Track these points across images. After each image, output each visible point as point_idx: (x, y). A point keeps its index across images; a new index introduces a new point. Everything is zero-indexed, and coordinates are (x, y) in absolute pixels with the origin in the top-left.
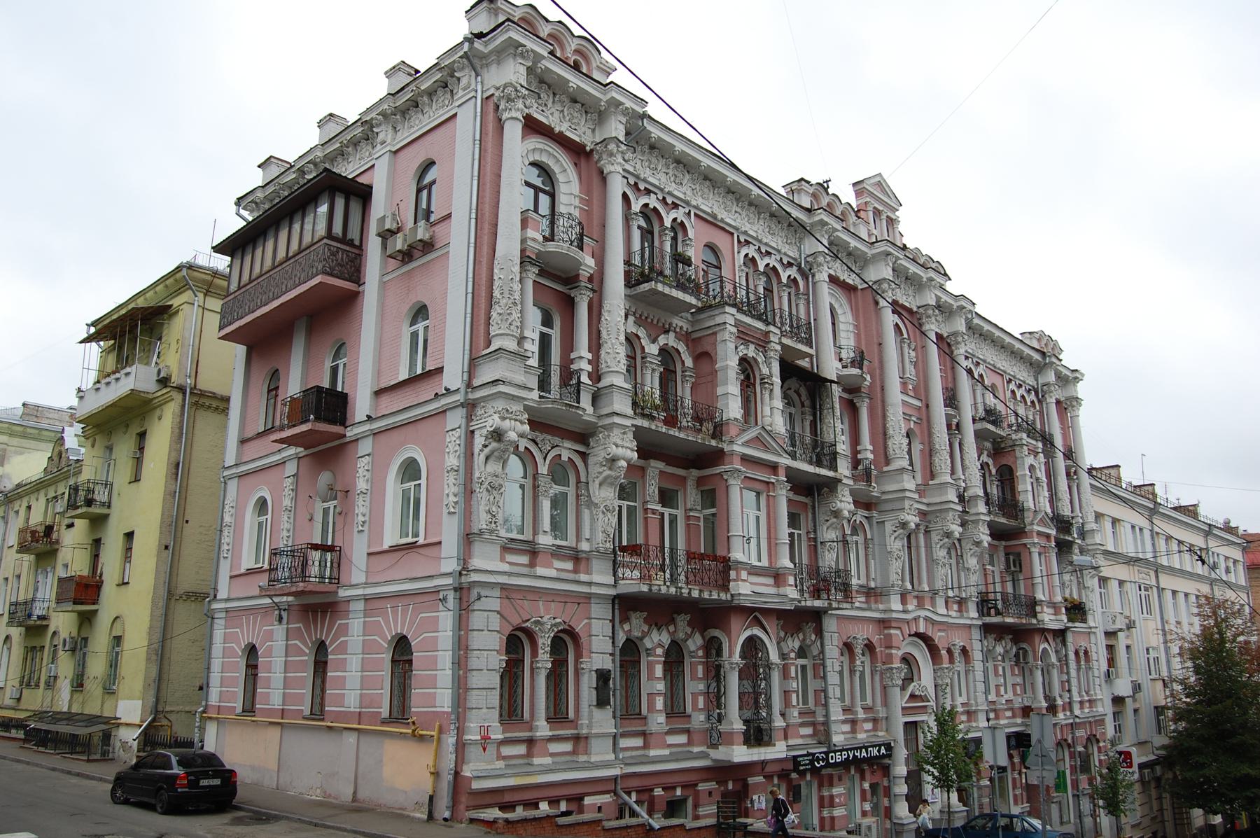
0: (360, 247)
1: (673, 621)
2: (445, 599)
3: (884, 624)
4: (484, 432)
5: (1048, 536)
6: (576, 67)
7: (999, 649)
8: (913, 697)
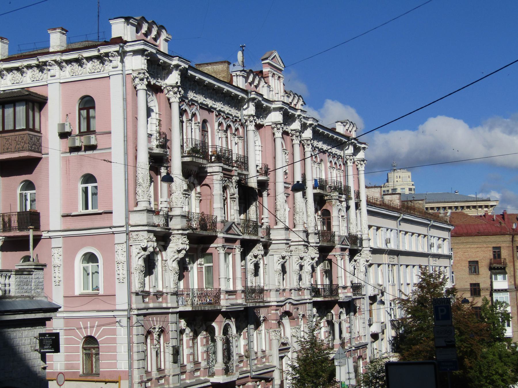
0: (39, 132)
2: (119, 322)
4: (139, 247)
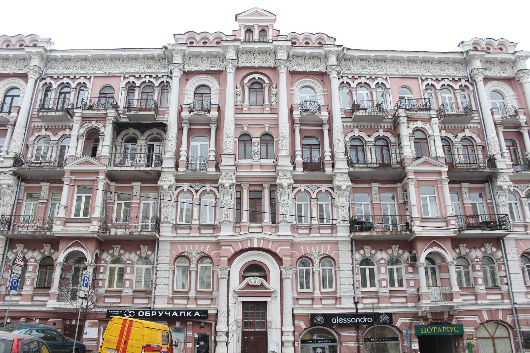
1: (43, 248)
3: (218, 244)
5: (440, 173)
6: (35, 45)
7: (382, 256)
8: (248, 286)
